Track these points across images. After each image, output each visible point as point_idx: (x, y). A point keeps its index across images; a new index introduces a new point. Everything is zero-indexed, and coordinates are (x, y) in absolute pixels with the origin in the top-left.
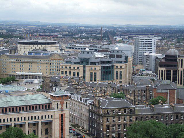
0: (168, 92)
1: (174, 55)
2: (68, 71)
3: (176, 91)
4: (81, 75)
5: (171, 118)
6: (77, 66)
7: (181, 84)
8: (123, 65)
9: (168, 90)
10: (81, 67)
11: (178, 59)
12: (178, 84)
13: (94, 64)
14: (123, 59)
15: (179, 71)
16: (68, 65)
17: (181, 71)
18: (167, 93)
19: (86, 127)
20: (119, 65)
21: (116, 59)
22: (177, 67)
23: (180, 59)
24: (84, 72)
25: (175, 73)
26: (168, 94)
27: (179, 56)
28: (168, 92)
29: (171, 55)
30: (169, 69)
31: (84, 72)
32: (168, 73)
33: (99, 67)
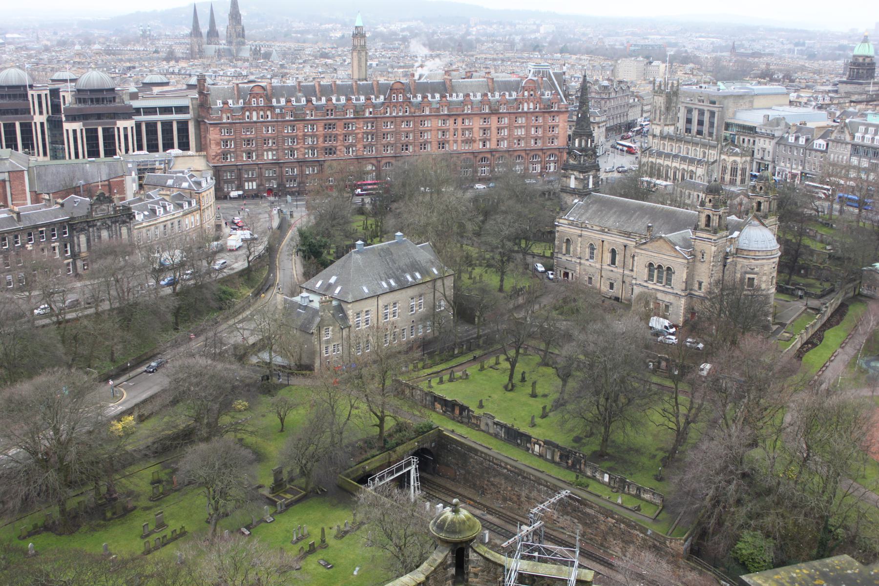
0: (7, 179)
1: (17, 84)
3: (26, 173)
5: (17, 242)
7: (45, 154)
9: (7, 174)
11: (30, 92)
12: (39, 155)
15: (35, 123)
17: (42, 124)
18: (4, 181)
22: (30, 113)
23: (35, 93)
25: (27, 129)
26: (8, 184)
27: (31, 87)
28: (7, 179)
29: (10, 84)
30: (9, 119)
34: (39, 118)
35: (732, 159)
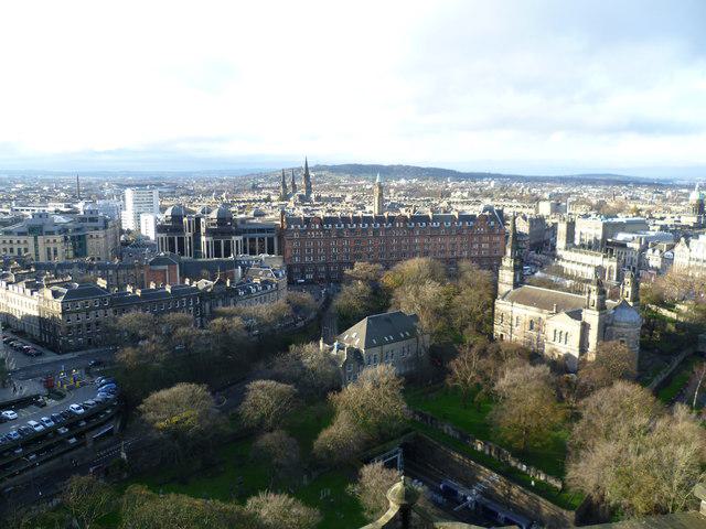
2: (8, 247)
4: (32, 251)
6: (22, 239)
8: (101, 233)
10: (30, 239)
13: (52, 233)
14: (100, 224)
16: (8, 238)
19: (36, 333)
20: (94, 233)
21: (88, 224)
24: (36, 245)
25: (181, 240)
31: (36, 245)
32: (171, 241)
33: (59, 238)
34: (188, 234)
35: (611, 263)
